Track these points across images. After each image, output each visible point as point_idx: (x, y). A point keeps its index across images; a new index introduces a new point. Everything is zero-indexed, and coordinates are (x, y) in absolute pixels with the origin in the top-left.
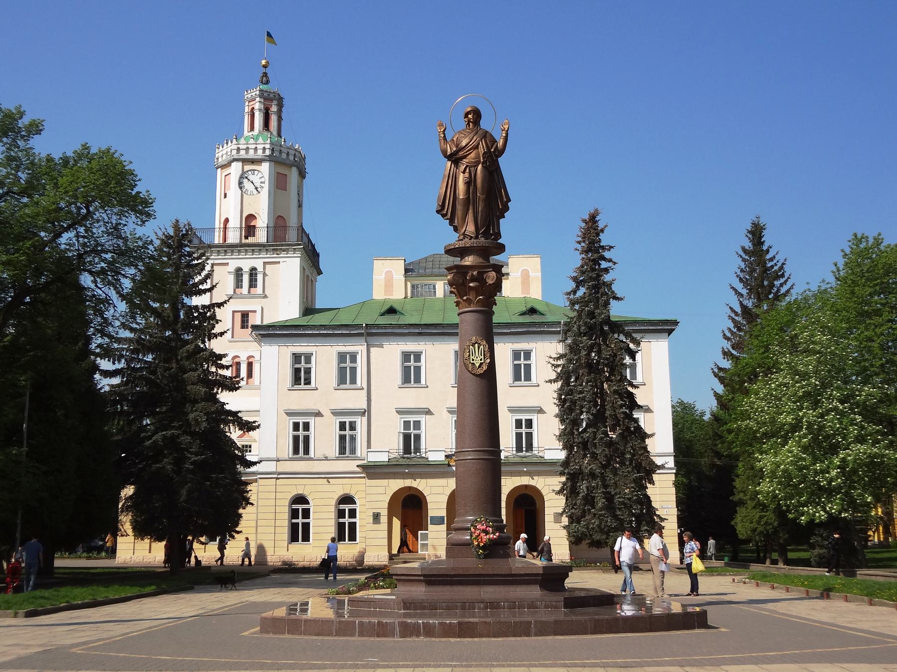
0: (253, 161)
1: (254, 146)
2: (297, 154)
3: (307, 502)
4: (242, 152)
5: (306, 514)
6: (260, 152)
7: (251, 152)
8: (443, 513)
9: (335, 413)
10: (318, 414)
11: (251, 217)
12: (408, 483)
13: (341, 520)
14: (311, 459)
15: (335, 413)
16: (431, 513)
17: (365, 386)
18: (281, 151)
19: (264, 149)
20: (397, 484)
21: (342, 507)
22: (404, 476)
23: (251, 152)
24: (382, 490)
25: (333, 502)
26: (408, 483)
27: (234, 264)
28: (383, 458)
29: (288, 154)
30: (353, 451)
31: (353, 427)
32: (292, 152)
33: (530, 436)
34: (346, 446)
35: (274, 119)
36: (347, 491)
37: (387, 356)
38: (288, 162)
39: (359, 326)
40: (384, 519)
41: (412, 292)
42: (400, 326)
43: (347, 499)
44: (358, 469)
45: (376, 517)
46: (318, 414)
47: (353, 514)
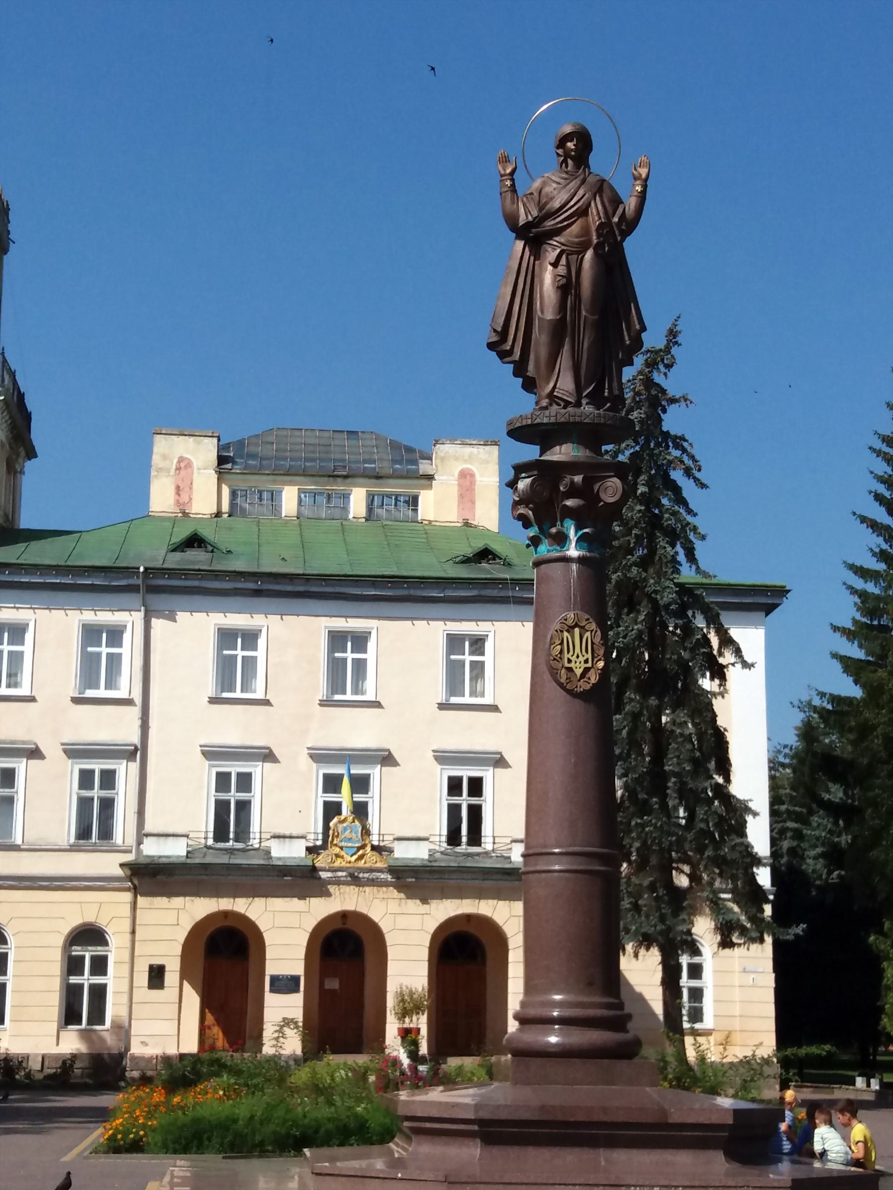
8: (297, 968)
9: (73, 752)
10: (35, 753)
12: (225, 904)
13: (74, 980)
14: (16, 848)
15: (73, 752)
17: (137, 696)
20: (201, 907)
21: (77, 951)
22: (216, 892)
24: (171, 917)
25: (60, 941)
26: (225, 904)
28: (176, 850)
30: (106, 833)
31: (108, 779)
33: (476, 813)
34: (94, 823)
36: (89, 917)
37: (188, 636)
39: (130, 571)
41: (233, 505)
42: (217, 575)
43: (90, 934)
44: (119, 872)
46: (35, 753)
47: (100, 966)
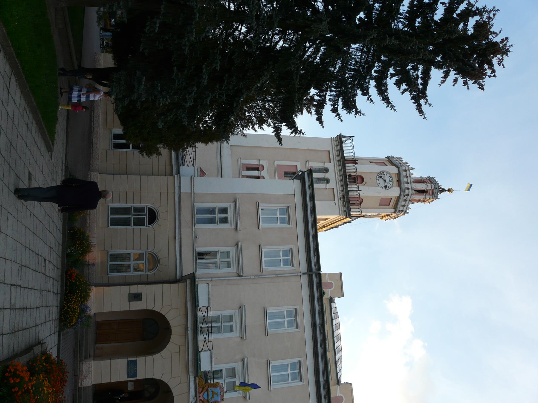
0: (399, 181)
1: (409, 181)
2: (403, 213)
3: (150, 223)
4: (404, 173)
5: (139, 222)
6: (406, 186)
7: (405, 180)
11: (362, 179)
16: (141, 361)
18: (406, 200)
19: (408, 189)
23: (405, 180)
27: (330, 166)
29: (404, 206)
32: (405, 208)
35: (421, 197)
38: (399, 205)
40: (135, 306)
45: (137, 297)
